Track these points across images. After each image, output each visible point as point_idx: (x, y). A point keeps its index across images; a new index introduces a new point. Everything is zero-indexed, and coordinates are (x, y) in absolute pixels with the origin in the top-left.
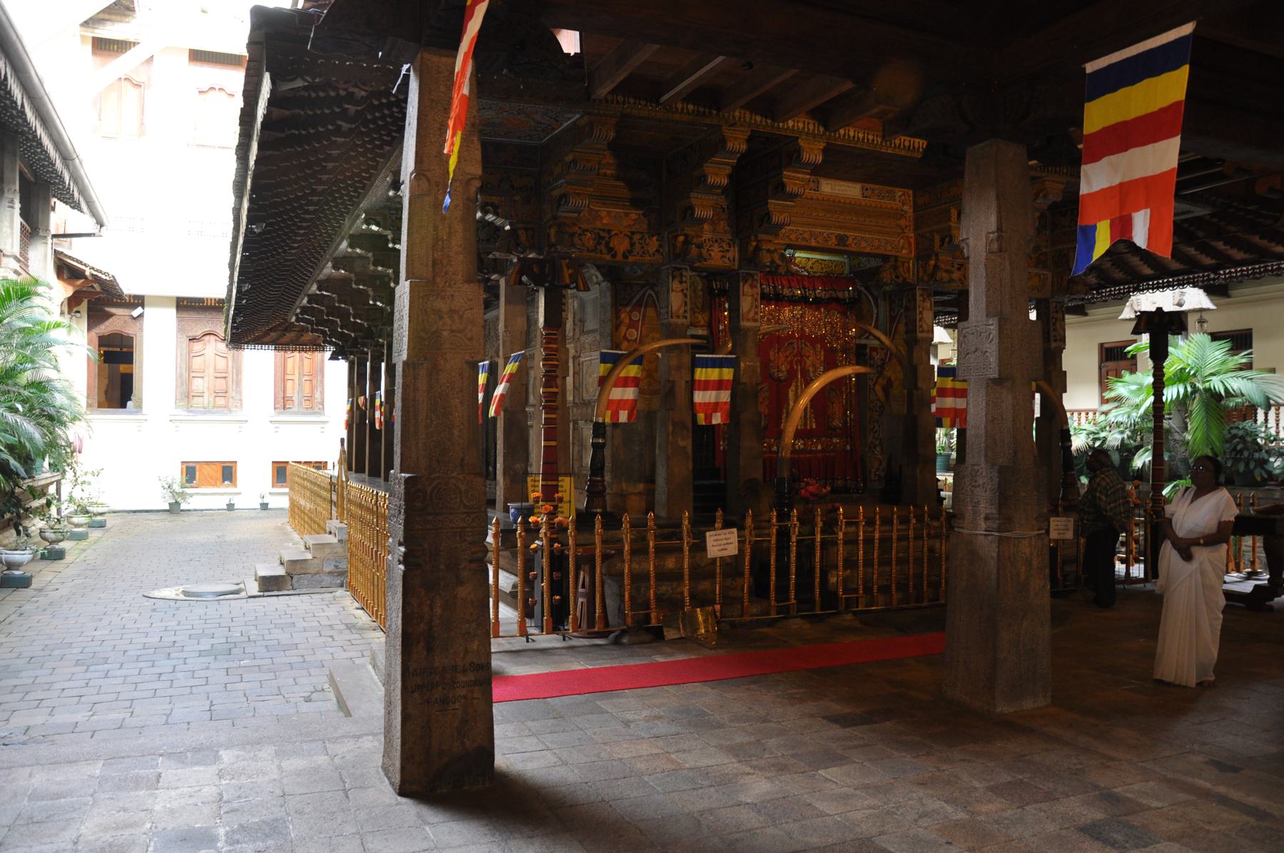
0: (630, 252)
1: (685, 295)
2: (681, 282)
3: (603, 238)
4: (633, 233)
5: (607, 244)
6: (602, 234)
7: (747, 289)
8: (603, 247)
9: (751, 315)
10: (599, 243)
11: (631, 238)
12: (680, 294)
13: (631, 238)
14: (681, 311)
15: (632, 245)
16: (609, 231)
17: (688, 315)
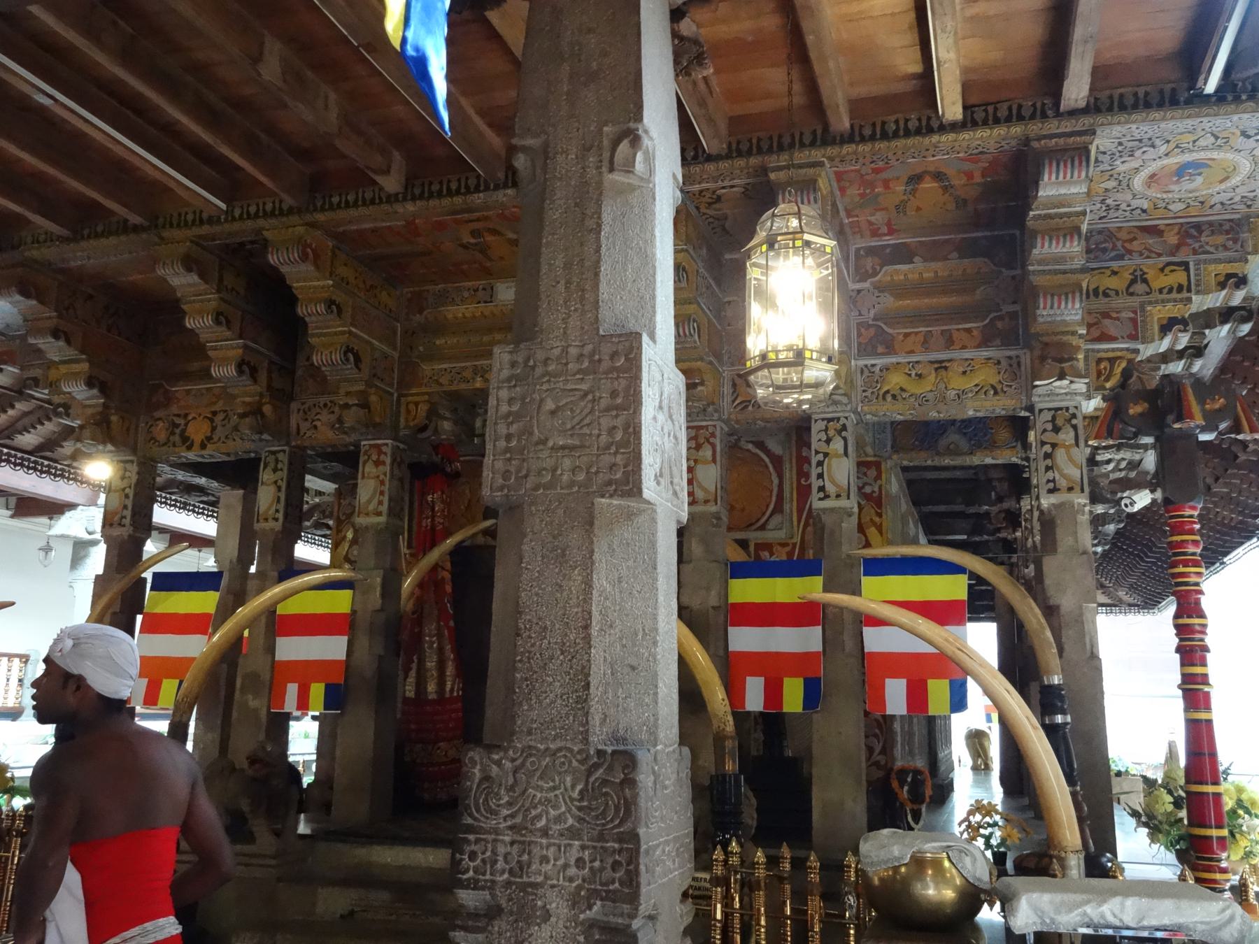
0: (209, 439)
1: (279, 489)
2: (275, 470)
3: (177, 426)
4: (215, 413)
5: (184, 431)
6: (177, 421)
7: (370, 468)
8: (177, 438)
9: (371, 507)
10: (173, 433)
11: (212, 420)
12: (272, 489)
13: (212, 420)
14: (272, 511)
15: (214, 429)
16: (186, 415)
17: (280, 516)
